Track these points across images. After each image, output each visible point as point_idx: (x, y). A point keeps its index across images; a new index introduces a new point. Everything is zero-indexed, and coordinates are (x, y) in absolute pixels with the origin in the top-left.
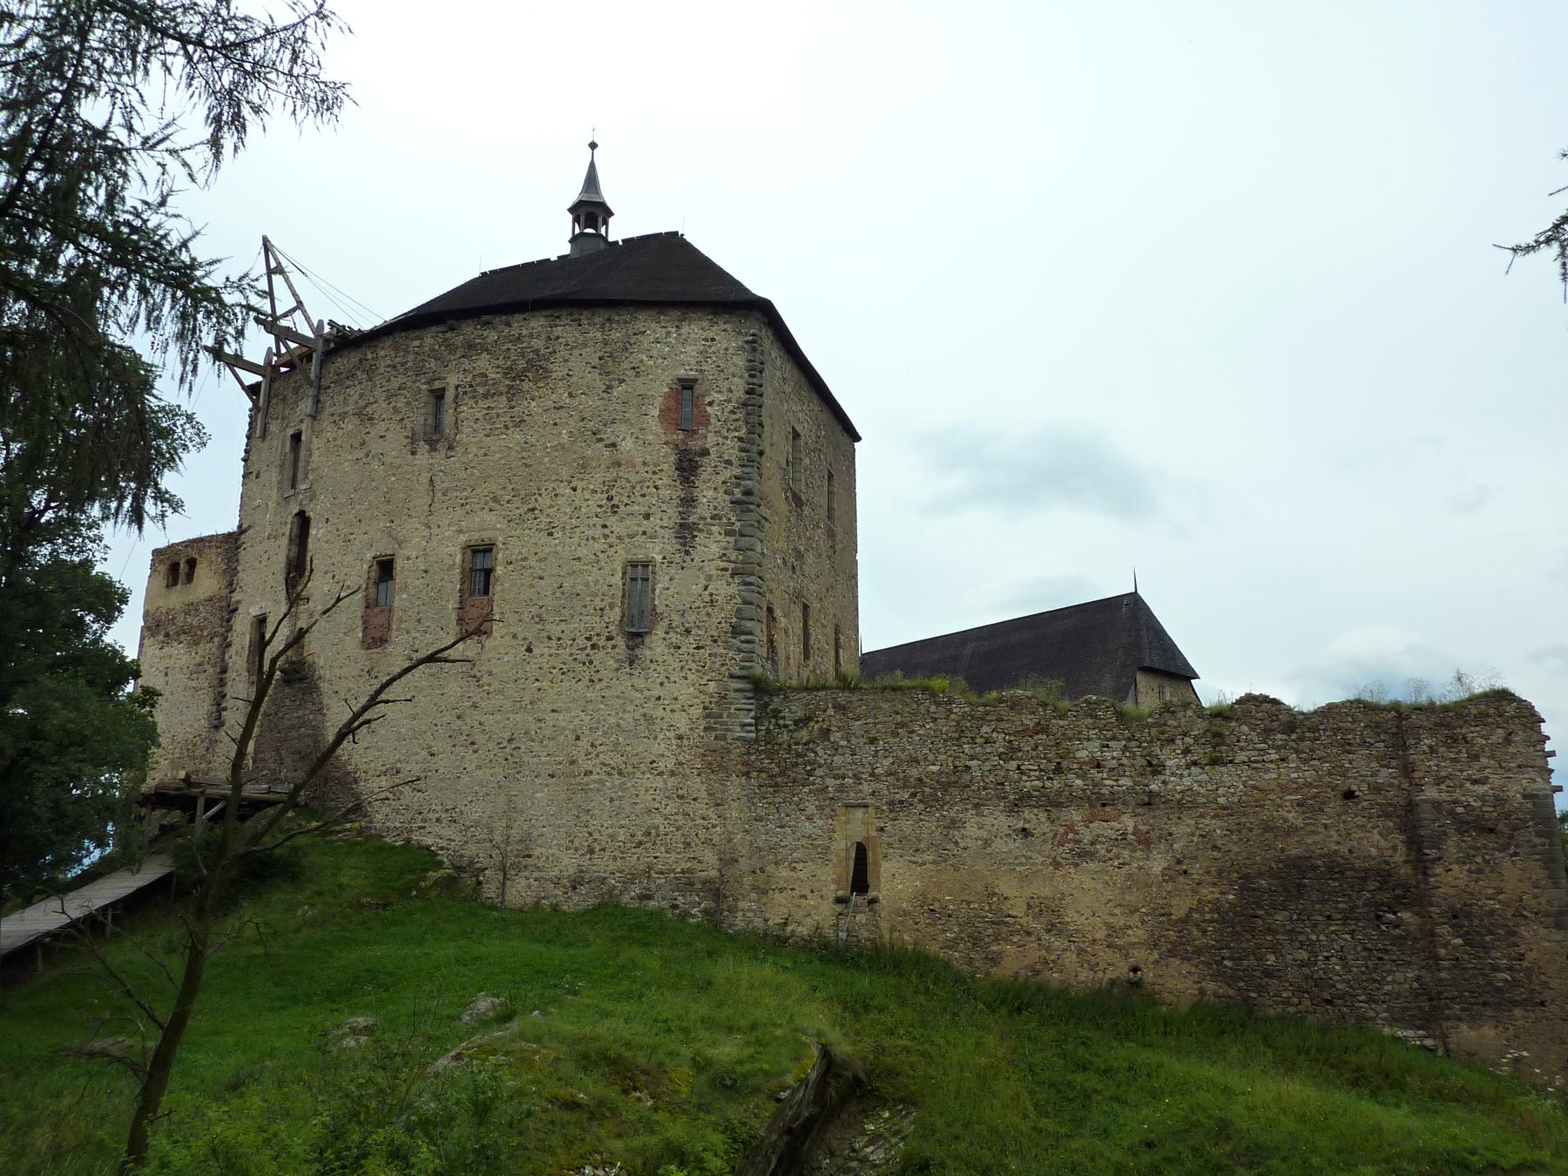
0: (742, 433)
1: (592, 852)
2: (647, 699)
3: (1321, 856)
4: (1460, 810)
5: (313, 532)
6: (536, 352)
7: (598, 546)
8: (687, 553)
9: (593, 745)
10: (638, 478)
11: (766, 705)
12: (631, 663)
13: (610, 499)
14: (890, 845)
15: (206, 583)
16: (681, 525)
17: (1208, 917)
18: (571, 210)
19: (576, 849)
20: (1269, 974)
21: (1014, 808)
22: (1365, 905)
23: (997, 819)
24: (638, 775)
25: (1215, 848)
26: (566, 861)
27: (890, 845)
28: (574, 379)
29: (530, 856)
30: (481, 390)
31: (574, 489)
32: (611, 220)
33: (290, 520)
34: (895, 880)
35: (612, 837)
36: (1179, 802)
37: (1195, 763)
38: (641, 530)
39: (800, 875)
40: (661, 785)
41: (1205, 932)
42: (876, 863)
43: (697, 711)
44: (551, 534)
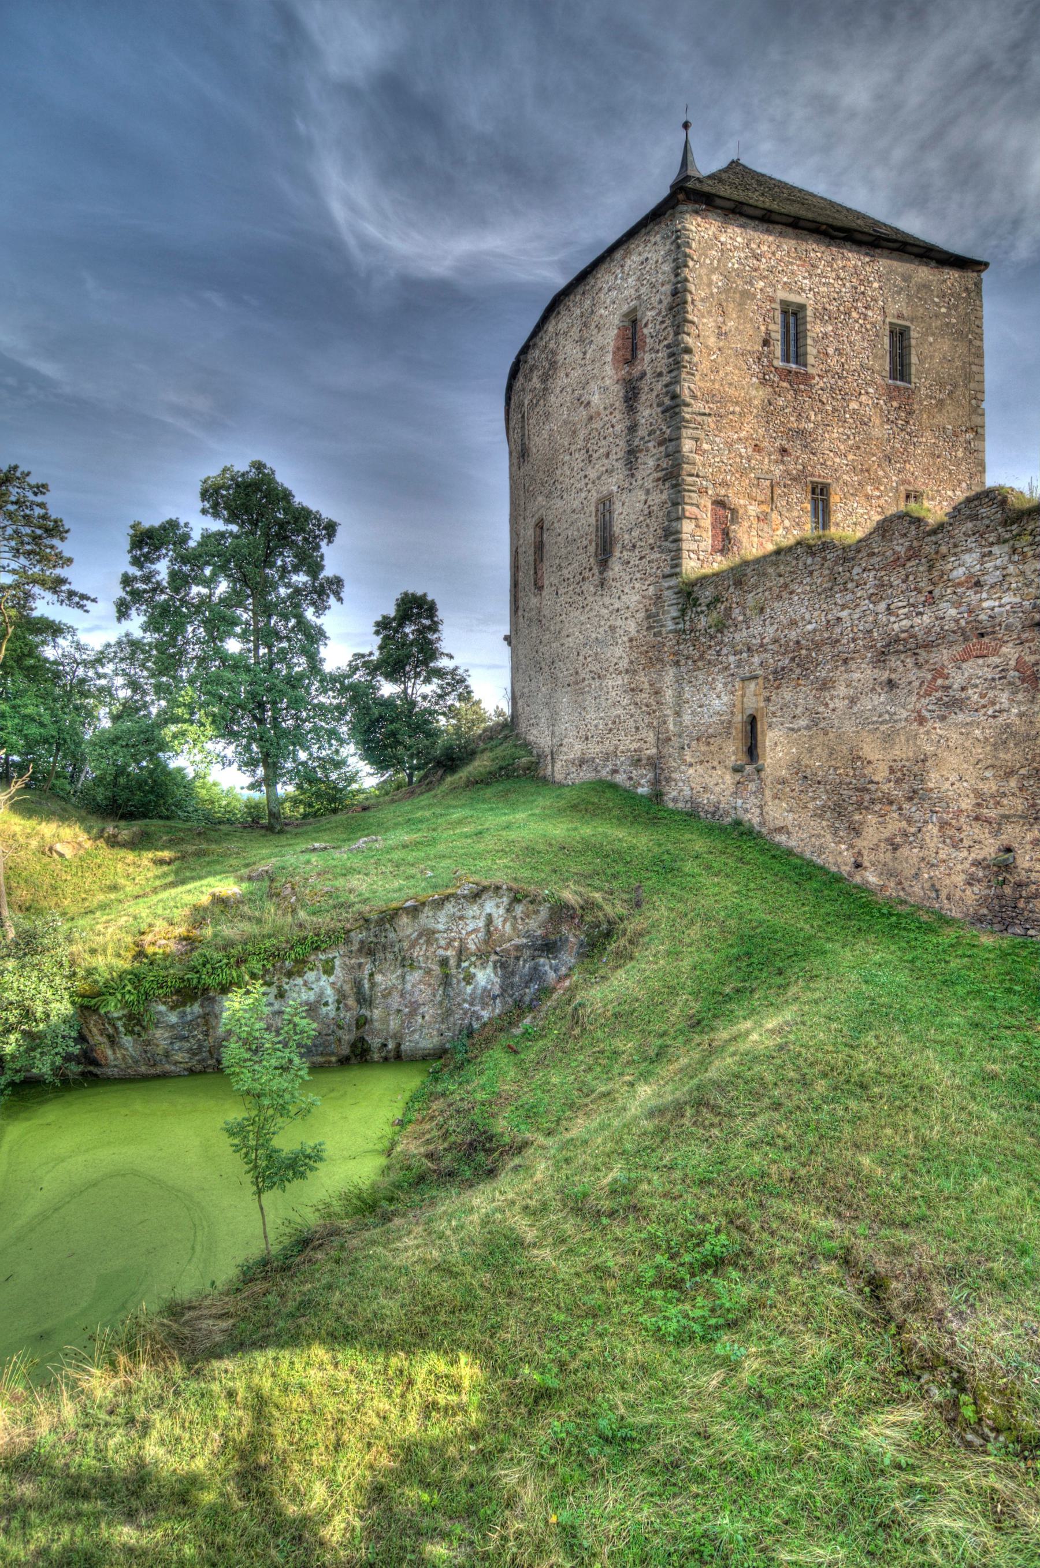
1: (587, 739)
7: (583, 495)
8: (633, 475)
14: (773, 713)
21: (881, 658)
23: (863, 673)
34: (778, 748)
40: (620, 682)
43: (641, 615)
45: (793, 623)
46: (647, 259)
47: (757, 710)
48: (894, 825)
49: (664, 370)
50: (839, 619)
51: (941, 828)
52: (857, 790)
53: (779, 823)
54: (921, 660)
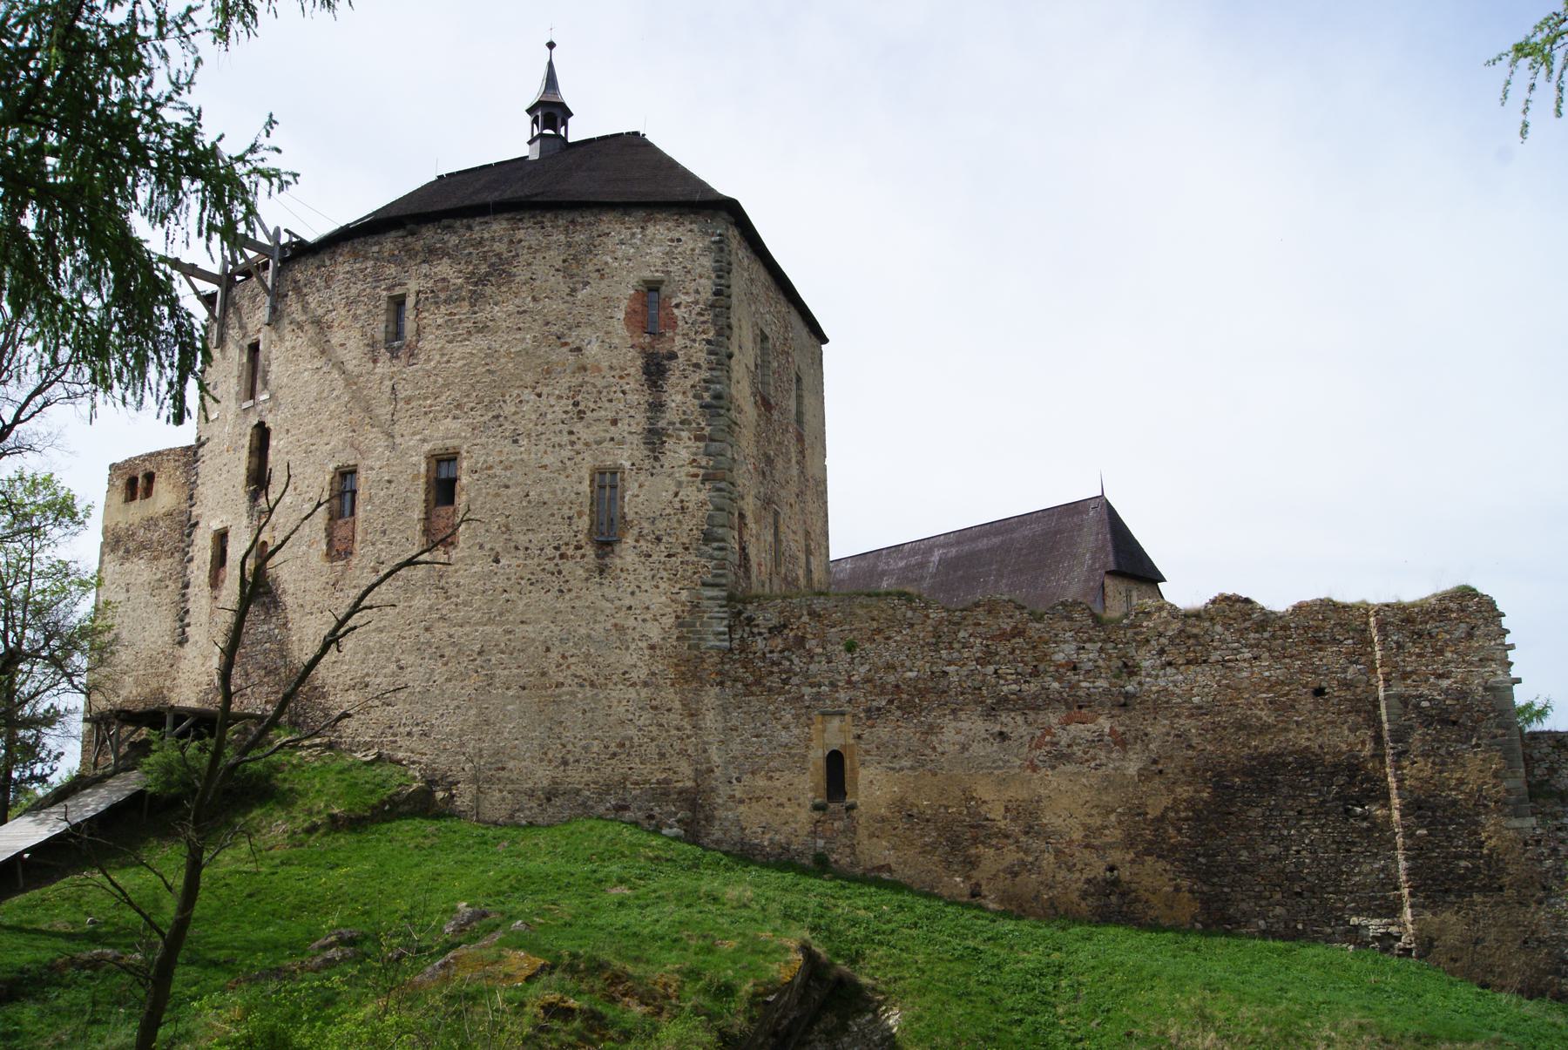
0: (711, 335)
1: (565, 763)
2: (618, 609)
3: (1291, 753)
4: (1425, 704)
5: (273, 443)
6: (499, 255)
7: (567, 452)
8: (656, 459)
9: (563, 657)
10: (604, 382)
11: (740, 613)
12: (601, 572)
13: (576, 404)
14: (867, 752)
15: (165, 497)
16: (650, 431)
17: (1183, 815)
18: (530, 111)
19: (550, 761)
20: (1242, 869)
22: (1334, 799)
23: (974, 724)
24: (611, 685)
25: (1190, 747)
26: (540, 773)
27: (867, 752)
28: (538, 283)
29: (503, 769)
30: (443, 296)
31: (539, 395)
32: (570, 121)
33: (249, 431)
34: (873, 786)
35: (586, 748)
36: (1155, 701)
37: (1170, 664)
38: (608, 436)
39: (777, 784)
41: (1179, 830)
42: (853, 770)
43: (669, 621)
44: (516, 441)
45: (890, 667)
46: (679, 240)
47: (844, 746)
48: (1011, 856)
49: (704, 366)
50: (945, 673)
51: (1056, 857)
52: (972, 826)
53: (876, 862)
54: (1030, 719)
